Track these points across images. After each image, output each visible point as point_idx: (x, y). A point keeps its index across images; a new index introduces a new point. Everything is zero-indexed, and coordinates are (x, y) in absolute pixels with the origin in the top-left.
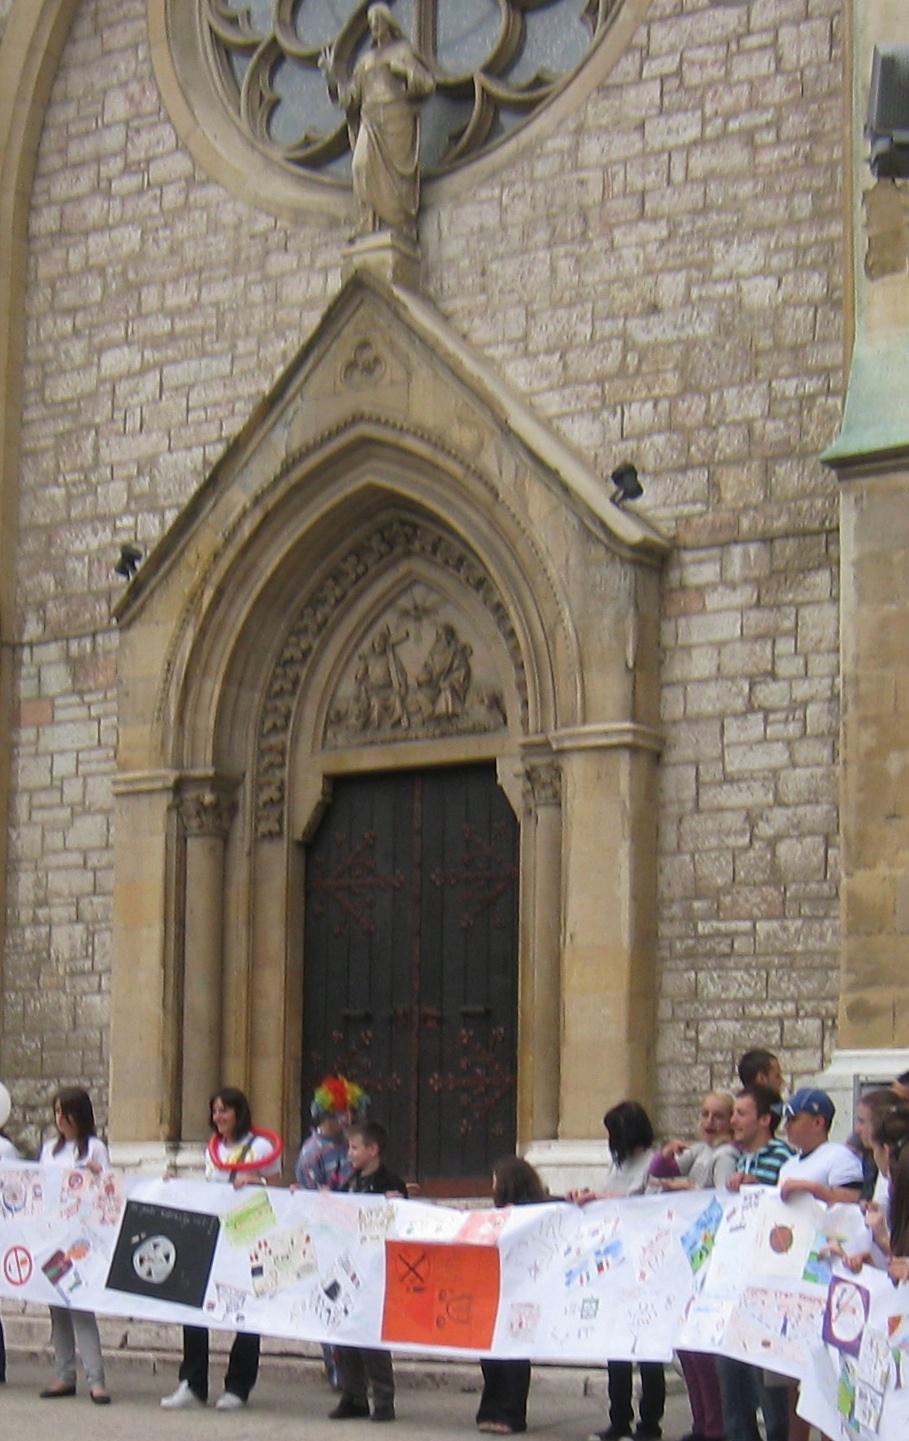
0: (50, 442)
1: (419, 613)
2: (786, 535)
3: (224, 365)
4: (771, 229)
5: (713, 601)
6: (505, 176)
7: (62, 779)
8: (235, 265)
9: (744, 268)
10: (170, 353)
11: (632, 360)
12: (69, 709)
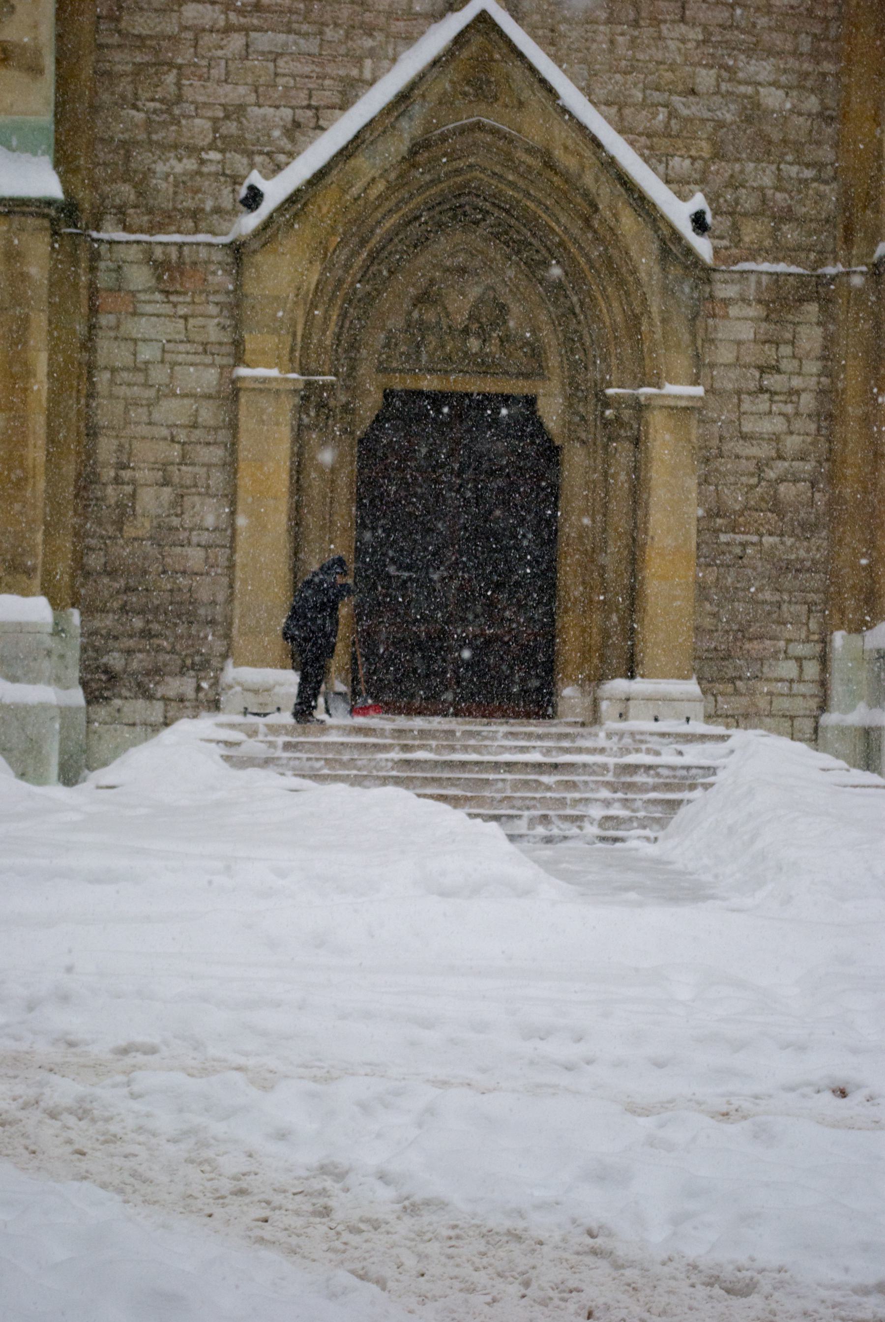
0: (129, 68)
3: (311, 46)
5: (733, 311)
7: (147, 363)
9: (760, 78)
10: (255, 22)
12: (155, 304)
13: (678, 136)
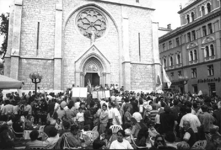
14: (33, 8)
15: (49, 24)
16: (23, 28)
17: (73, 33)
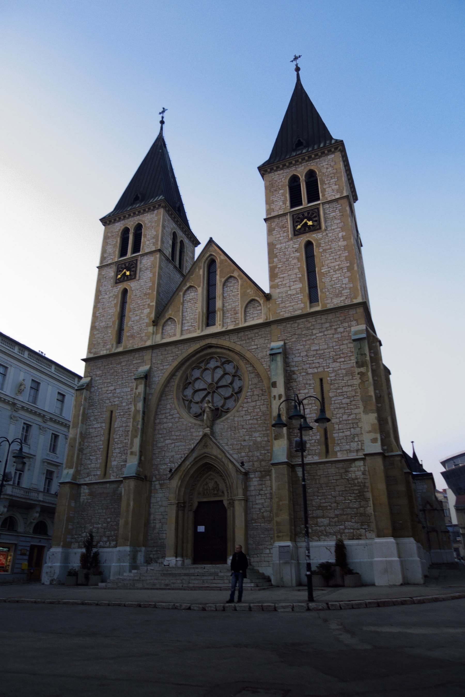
0: (157, 452)
1: (212, 479)
2: (263, 471)
4: (260, 431)
5: (254, 480)
6: (225, 421)
8: (186, 430)
9: (256, 436)
11: (242, 447)
13: (243, 449)
14: (105, 387)
15: (128, 410)
16: (89, 428)
17: (170, 417)
